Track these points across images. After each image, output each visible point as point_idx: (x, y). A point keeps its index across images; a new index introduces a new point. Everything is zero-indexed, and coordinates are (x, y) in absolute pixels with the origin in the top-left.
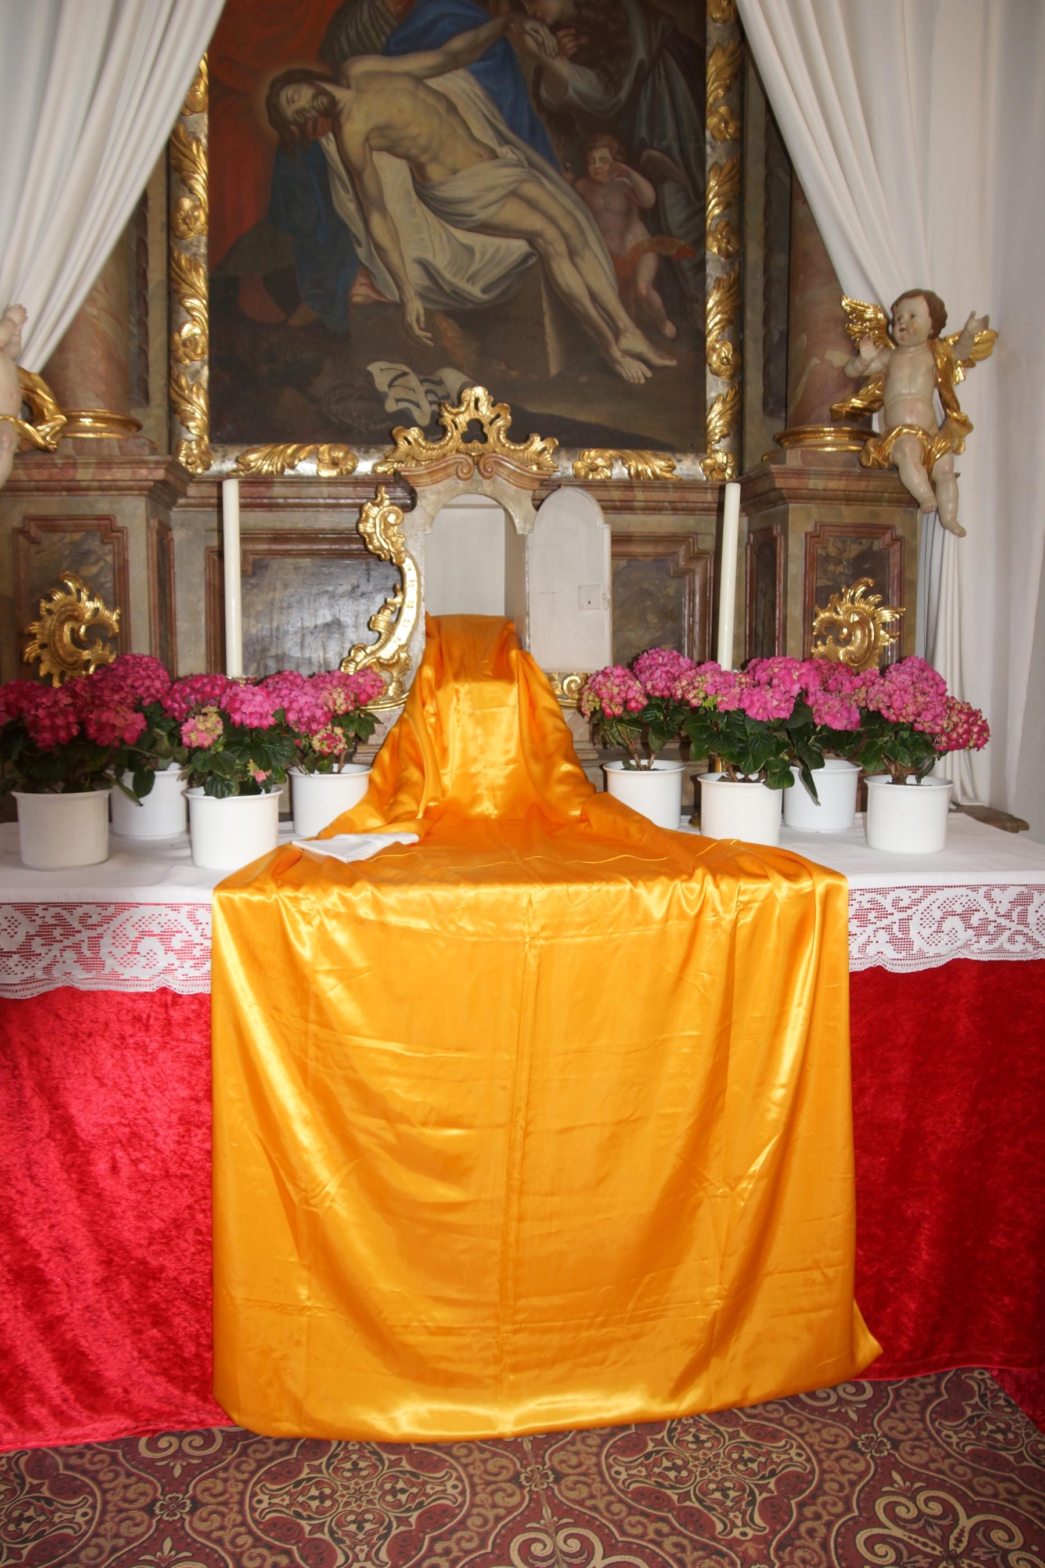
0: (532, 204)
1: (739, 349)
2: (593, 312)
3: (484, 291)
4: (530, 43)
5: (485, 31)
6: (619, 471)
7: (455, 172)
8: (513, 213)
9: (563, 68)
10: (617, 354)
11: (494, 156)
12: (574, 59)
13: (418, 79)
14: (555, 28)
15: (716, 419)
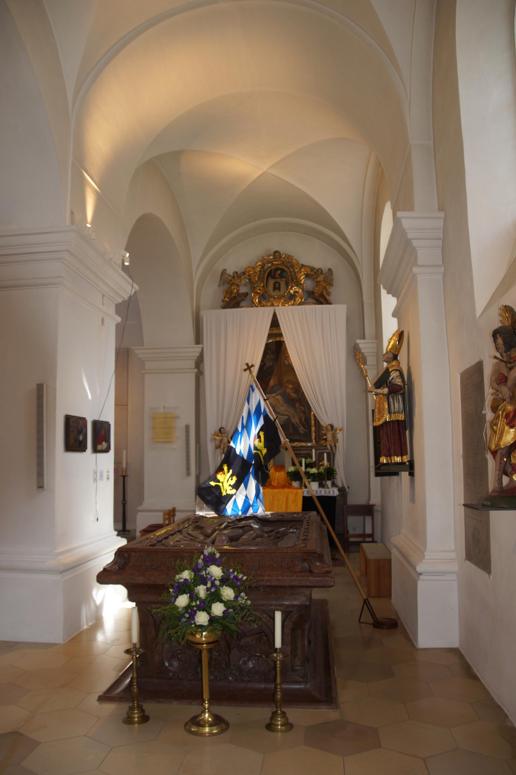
0: (288, 411)
1: (315, 428)
2: (296, 425)
3: (283, 423)
4: (288, 391)
5: (282, 390)
6: (300, 445)
7: (278, 408)
8: (286, 413)
9: (292, 394)
10: (299, 430)
11: (283, 406)
12: (294, 393)
13: (274, 397)
14: (291, 389)
15: (313, 437)
